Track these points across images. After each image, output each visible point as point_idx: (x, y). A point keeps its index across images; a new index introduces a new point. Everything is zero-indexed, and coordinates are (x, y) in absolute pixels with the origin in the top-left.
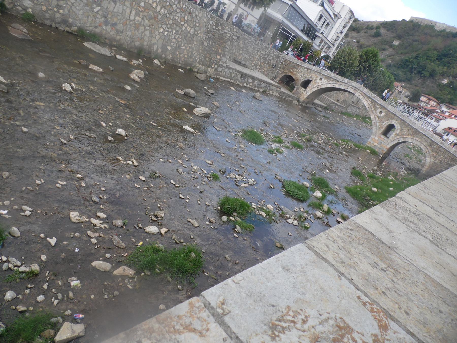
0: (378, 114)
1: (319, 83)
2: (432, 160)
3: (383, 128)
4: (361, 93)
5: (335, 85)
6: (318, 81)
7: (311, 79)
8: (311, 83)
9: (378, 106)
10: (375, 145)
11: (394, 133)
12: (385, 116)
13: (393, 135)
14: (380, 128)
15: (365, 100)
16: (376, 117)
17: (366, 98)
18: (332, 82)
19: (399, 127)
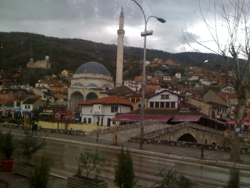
4: (191, 129)
9: (199, 132)
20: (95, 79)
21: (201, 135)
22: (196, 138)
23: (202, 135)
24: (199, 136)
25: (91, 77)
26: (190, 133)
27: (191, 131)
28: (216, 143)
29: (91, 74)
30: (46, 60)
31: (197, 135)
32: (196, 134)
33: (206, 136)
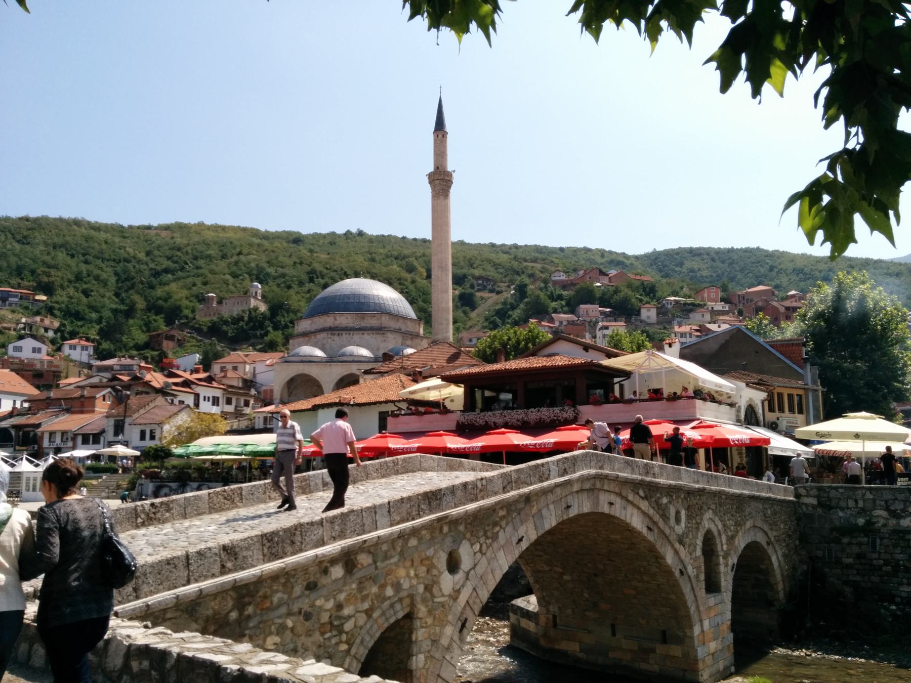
0: (676, 527)
1: (456, 594)
2: (780, 553)
3: (703, 567)
4: (612, 487)
5: (521, 532)
6: (447, 582)
7: (401, 615)
8: (420, 634)
9: (665, 500)
10: (713, 654)
11: (721, 559)
12: (689, 517)
13: (722, 569)
14: (697, 576)
15: (630, 509)
16: (677, 545)
17: (631, 497)
18: (509, 529)
19: (720, 526)
20: (361, 329)
21: (678, 513)
22: (649, 529)
23: (683, 513)
24: (665, 517)
25: (351, 325)
26: (606, 509)
27: (618, 501)
28: (764, 543)
29: (348, 316)
30: (254, 294)
31: (657, 518)
32: (644, 513)
33: (709, 514)
